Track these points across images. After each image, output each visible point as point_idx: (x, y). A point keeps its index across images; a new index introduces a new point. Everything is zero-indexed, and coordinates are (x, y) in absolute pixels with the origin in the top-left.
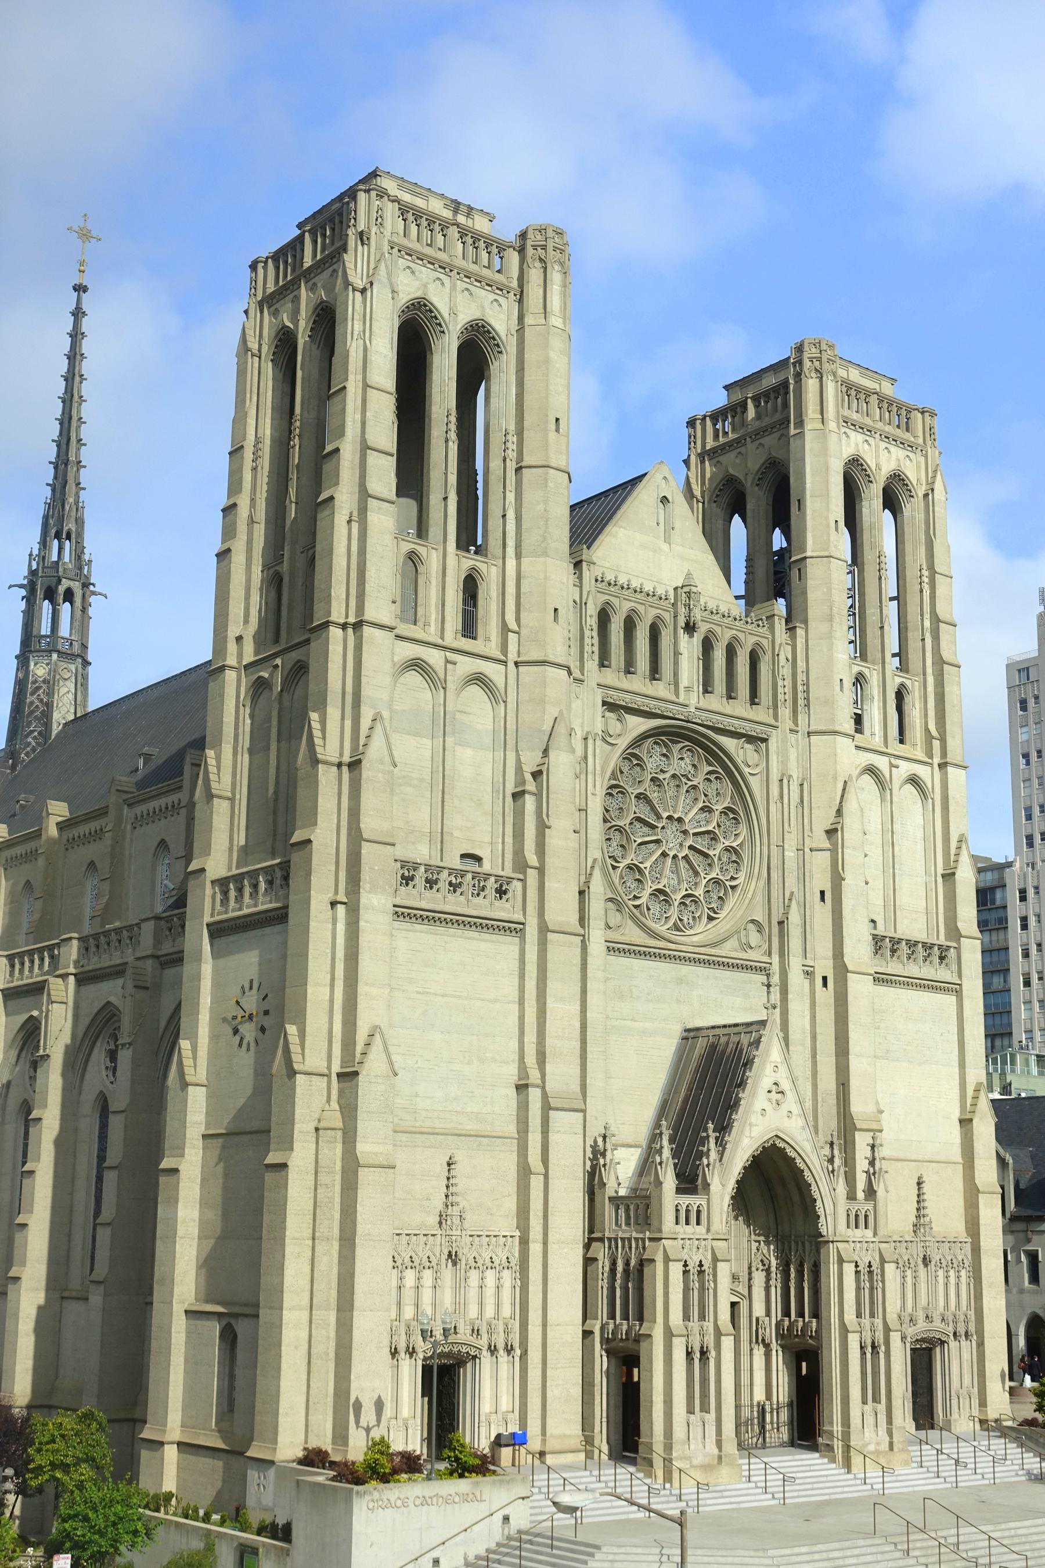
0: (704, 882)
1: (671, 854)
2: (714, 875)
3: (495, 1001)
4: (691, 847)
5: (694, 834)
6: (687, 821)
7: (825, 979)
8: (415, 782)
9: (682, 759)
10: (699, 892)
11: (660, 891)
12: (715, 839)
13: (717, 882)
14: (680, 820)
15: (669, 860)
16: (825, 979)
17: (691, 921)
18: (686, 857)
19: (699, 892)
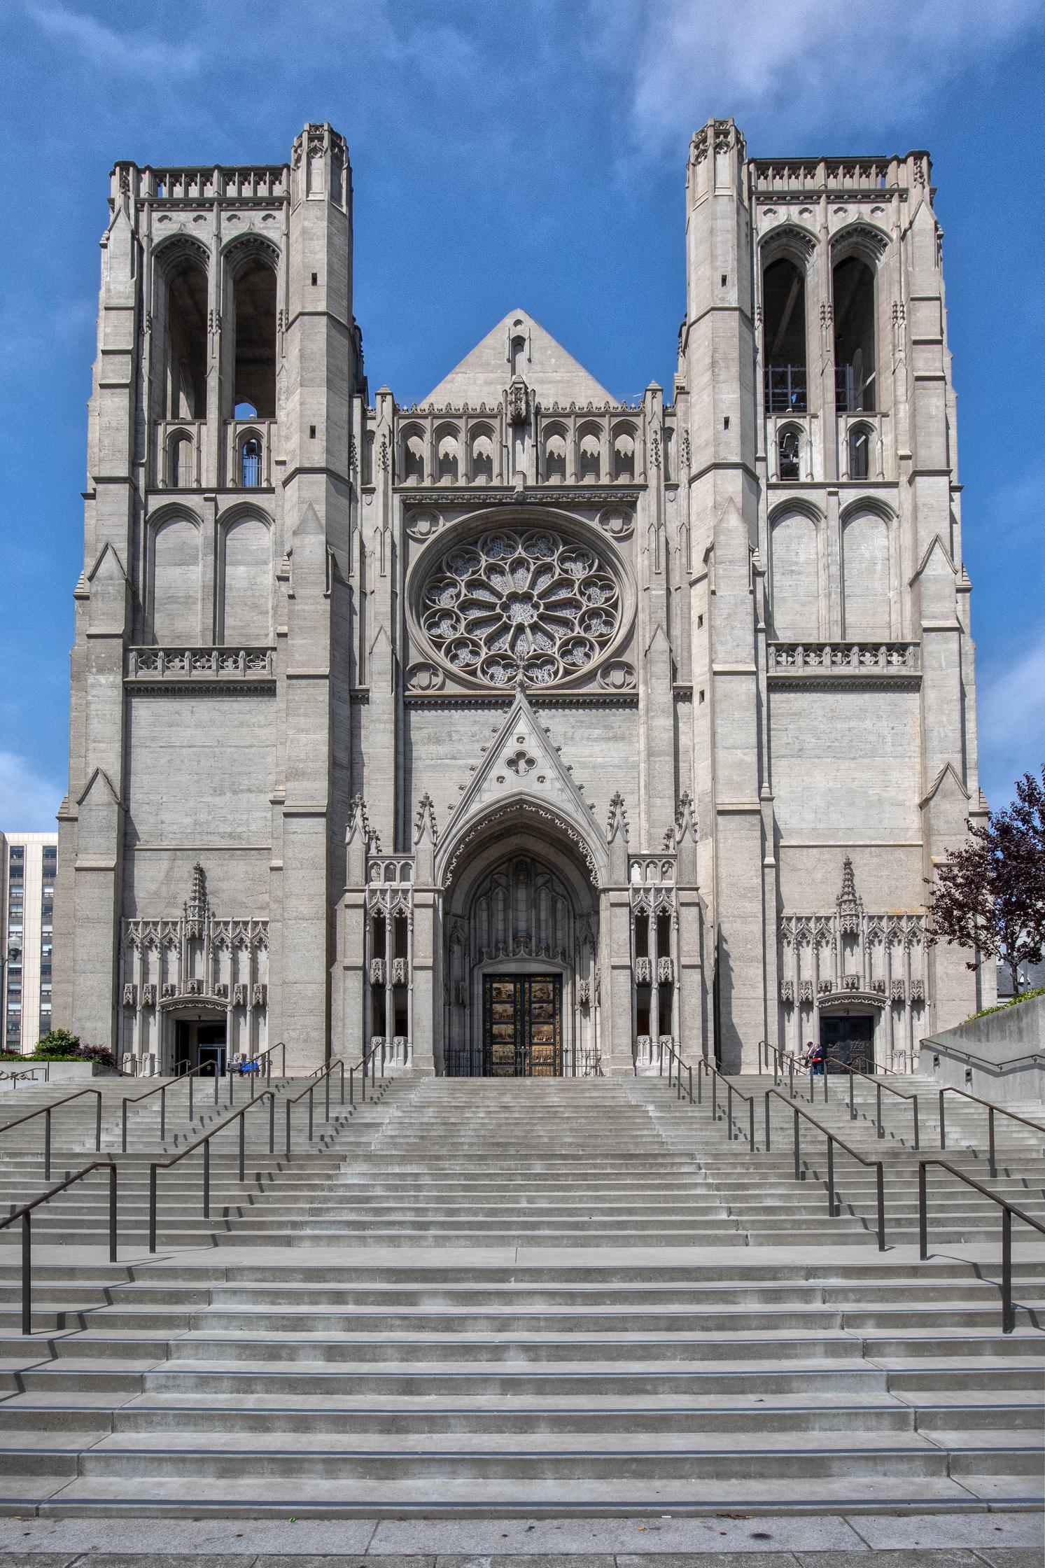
0: (558, 643)
1: (514, 624)
2: (575, 634)
3: (251, 746)
4: (541, 617)
5: (548, 607)
6: (535, 593)
7: (702, 694)
8: (182, 600)
9: (534, 546)
10: (554, 651)
11: (504, 657)
12: (578, 607)
13: (580, 642)
14: (526, 598)
15: (513, 629)
16: (702, 694)
17: (546, 677)
18: (535, 628)
19: (554, 651)
